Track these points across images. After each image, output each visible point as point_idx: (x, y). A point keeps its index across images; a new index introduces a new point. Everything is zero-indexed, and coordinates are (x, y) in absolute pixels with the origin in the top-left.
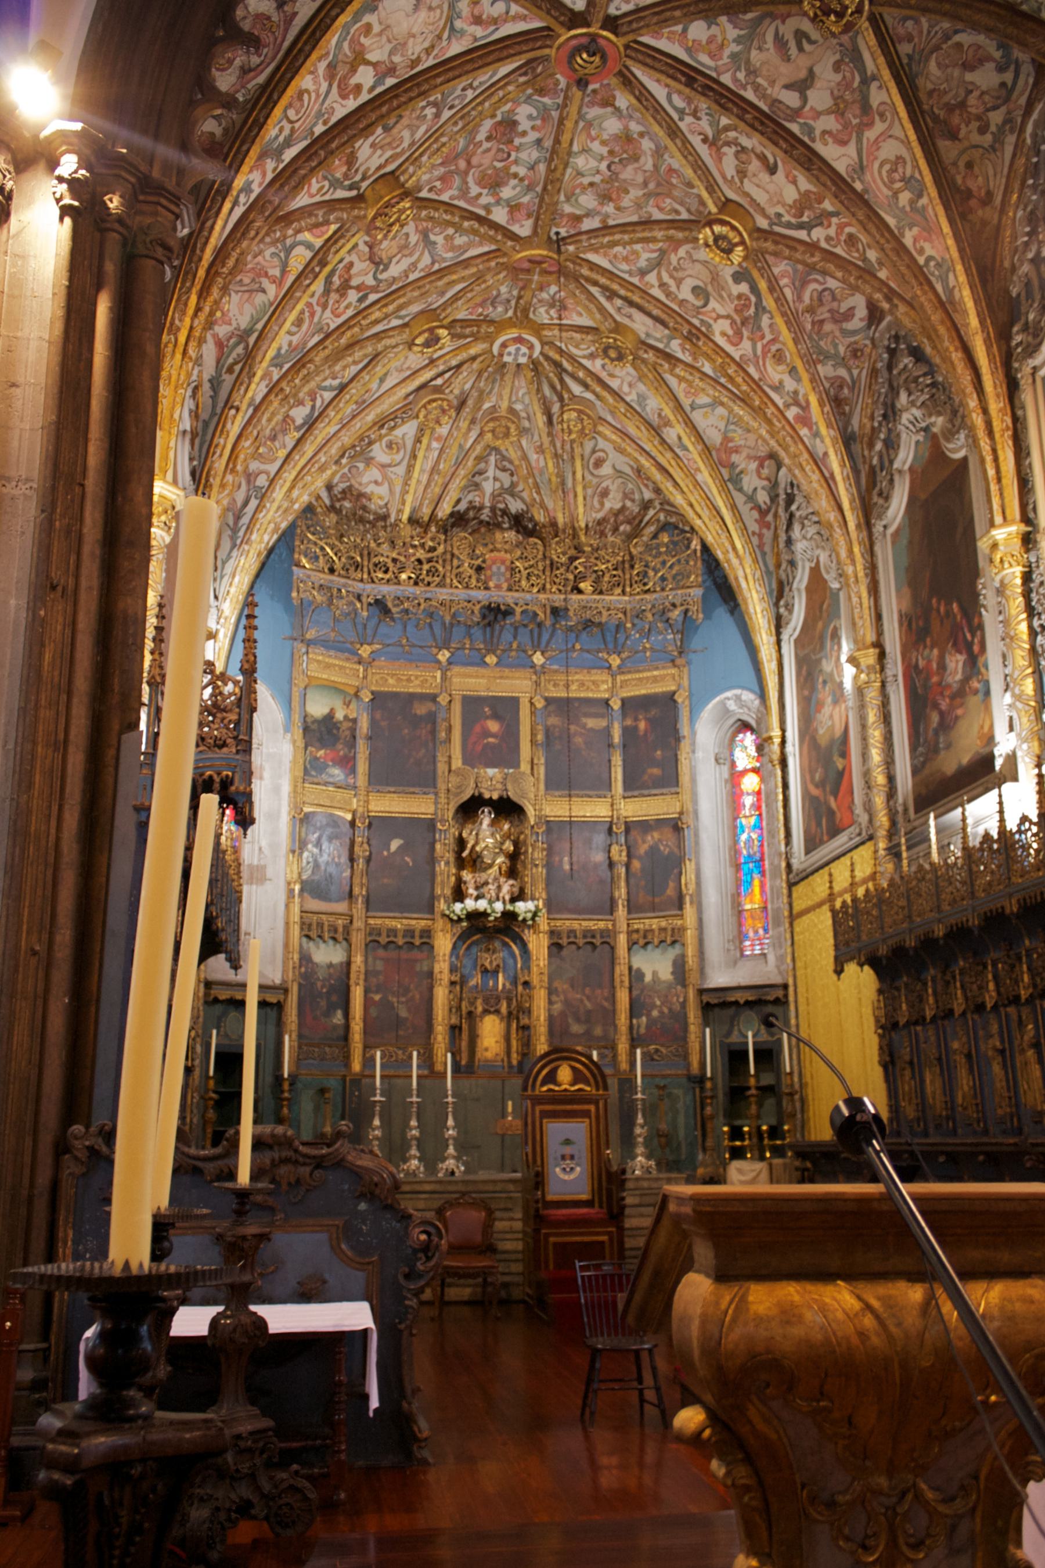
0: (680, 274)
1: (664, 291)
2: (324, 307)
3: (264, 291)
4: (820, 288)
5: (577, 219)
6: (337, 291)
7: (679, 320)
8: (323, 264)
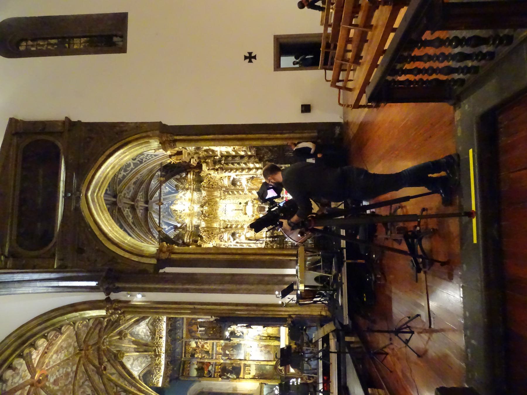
5: (75, 348)
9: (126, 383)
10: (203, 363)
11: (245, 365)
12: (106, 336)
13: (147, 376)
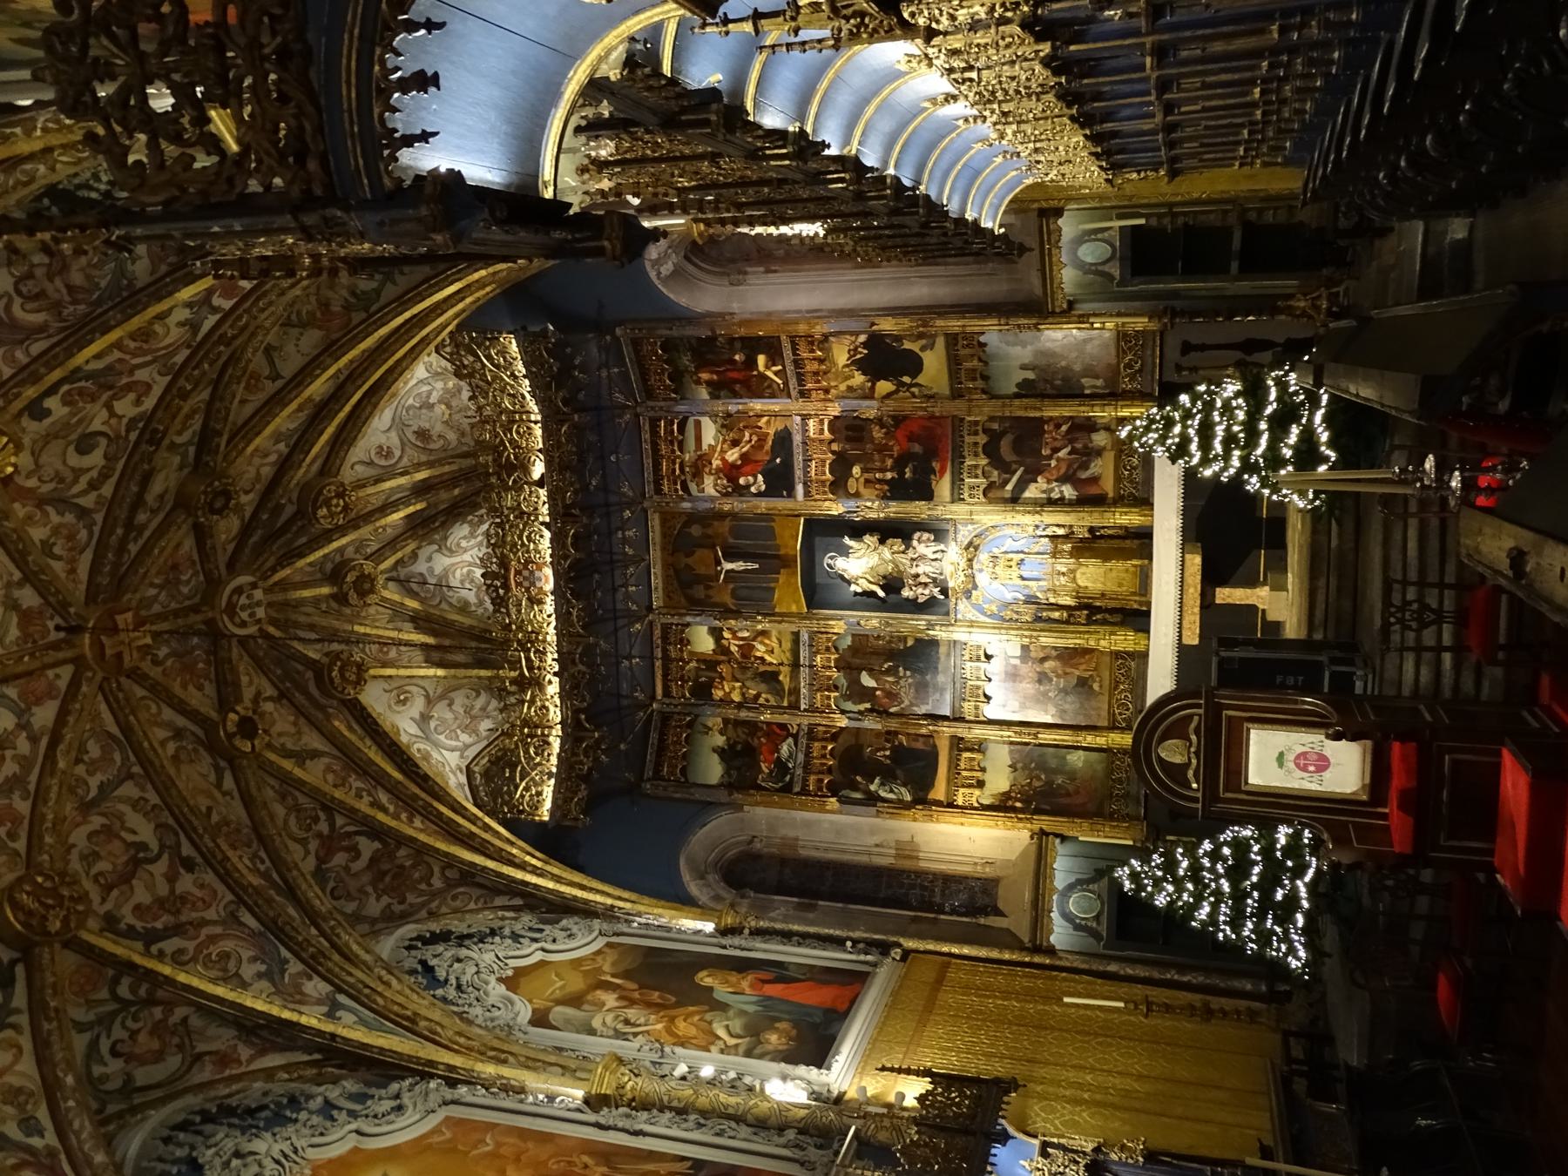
0: (69, 476)
1: (103, 483)
2: (205, 923)
3: (185, 1020)
4: (18, 301)
5: (26, 617)
6: (178, 912)
7: (136, 457)
8: (132, 966)
9: (383, 797)
10: (753, 726)
11: (958, 744)
12: (248, 579)
13: (497, 772)
